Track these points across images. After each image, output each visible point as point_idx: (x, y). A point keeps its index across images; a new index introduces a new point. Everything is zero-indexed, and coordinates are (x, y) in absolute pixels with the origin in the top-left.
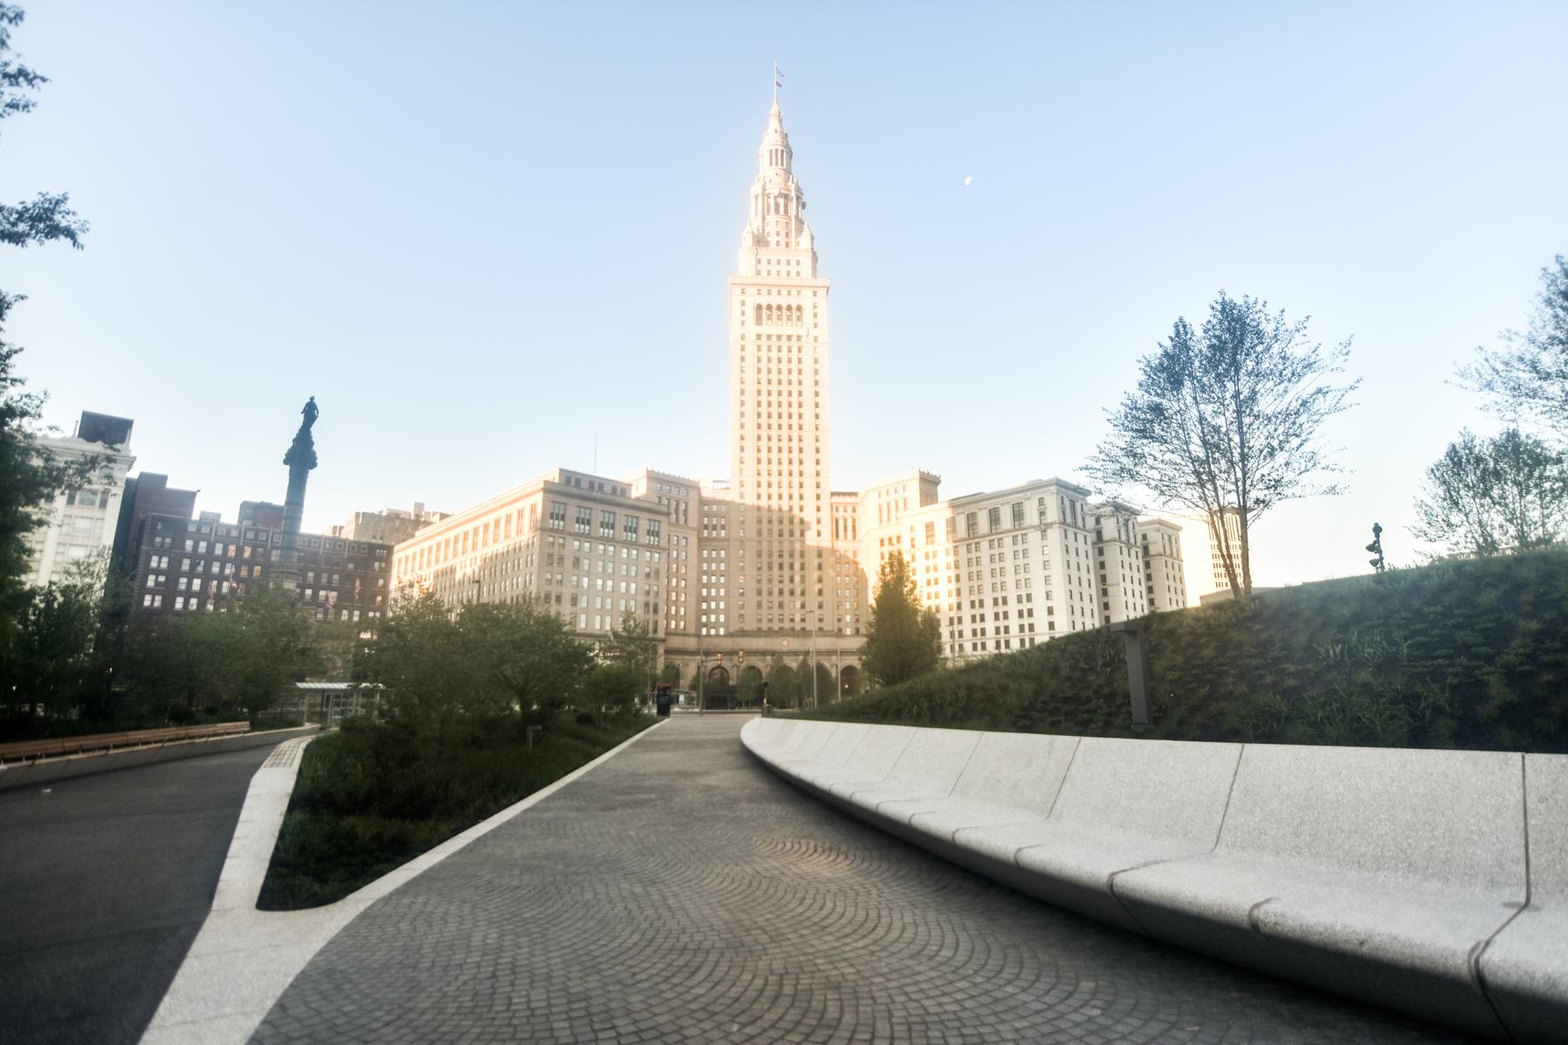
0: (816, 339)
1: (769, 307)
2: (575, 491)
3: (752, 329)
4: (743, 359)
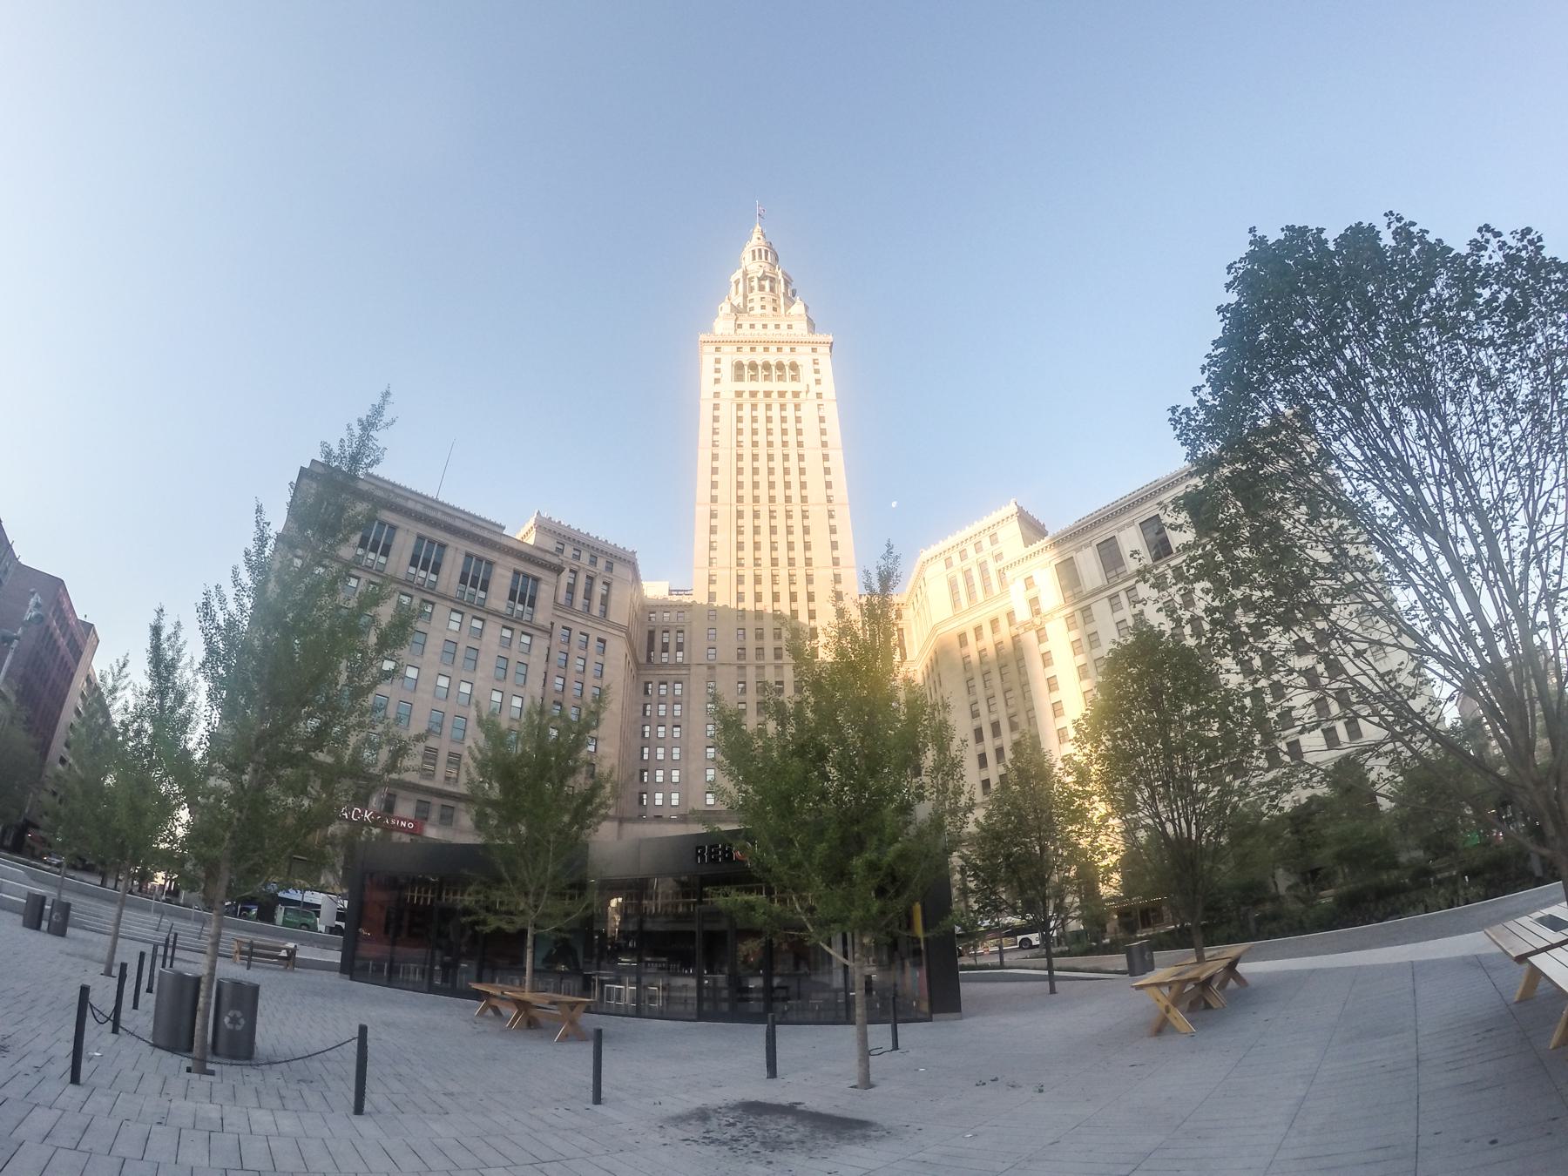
0: (819, 395)
1: (753, 366)
3: (728, 387)
4: (716, 419)
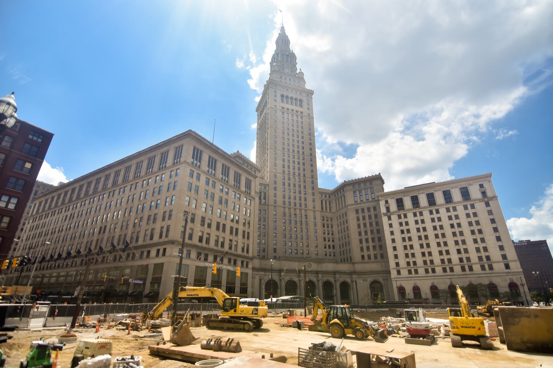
0: (309, 114)
1: (287, 97)
3: (280, 104)
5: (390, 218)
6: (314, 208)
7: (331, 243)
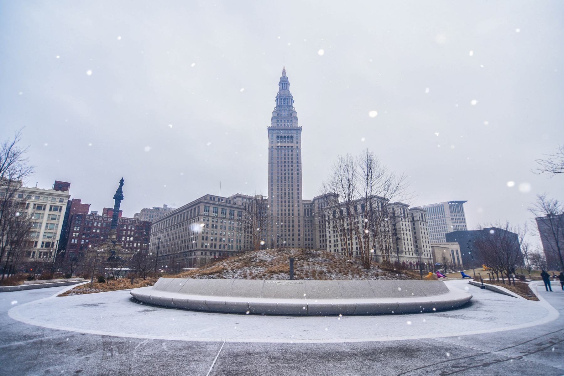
0: (297, 147)
2: (213, 202)
5: (329, 224)
6: (299, 214)
7: (310, 237)
